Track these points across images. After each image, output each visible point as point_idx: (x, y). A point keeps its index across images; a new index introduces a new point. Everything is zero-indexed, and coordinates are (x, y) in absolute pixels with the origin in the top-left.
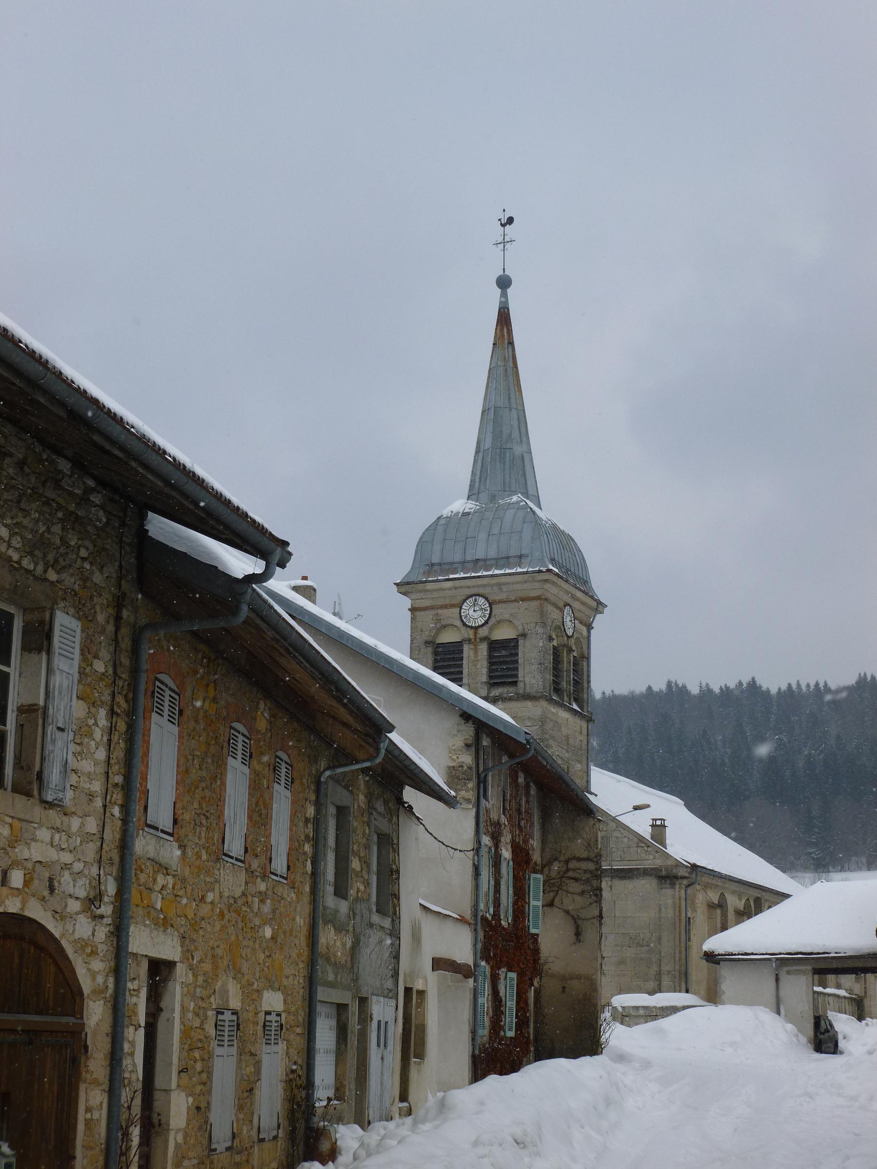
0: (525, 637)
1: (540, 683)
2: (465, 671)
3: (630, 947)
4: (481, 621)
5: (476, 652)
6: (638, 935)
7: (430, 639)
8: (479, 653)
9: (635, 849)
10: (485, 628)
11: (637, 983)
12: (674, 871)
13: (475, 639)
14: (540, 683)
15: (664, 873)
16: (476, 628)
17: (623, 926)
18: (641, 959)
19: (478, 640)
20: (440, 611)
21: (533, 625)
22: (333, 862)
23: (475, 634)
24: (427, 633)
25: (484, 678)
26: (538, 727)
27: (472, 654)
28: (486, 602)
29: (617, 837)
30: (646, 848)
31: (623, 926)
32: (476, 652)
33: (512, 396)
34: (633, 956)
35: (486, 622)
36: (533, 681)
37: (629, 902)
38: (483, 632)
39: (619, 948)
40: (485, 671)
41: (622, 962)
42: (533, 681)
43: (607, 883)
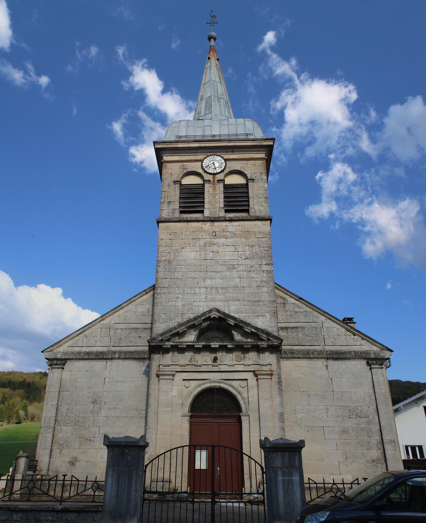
0: (253, 181)
1: (267, 210)
2: (206, 200)
3: (350, 418)
4: (218, 170)
5: (214, 189)
6: (356, 407)
7: (179, 180)
8: (217, 189)
9: (344, 337)
10: (221, 174)
11: (362, 451)
12: (381, 354)
13: (214, 181)
14: (267, 210)
15: (373, 356)
16: (214, 174)
17: (342, 400)
18: (361, 429)
19: (216, 182)
20: (185, 164)
21: (259, 174)
22: (254, 144)
23: (214, 178)
24: (176, 176)
25: (222, 205)
26: (267, 239)
27: (211, 189)
28: (222, 159)
29: (328, 328)
30: (353, 336)
31: (342, 400)
32: (214, 189)
33: (221, 78)
34: (354, 426)
35: (222, 171)
36: (262, 208)
37: (344, 379)
38: (218, 177)
39: (340, 419)
40: (222, 200)
41: (345, 431)
42: (262, 208)
43: (323, 363)
